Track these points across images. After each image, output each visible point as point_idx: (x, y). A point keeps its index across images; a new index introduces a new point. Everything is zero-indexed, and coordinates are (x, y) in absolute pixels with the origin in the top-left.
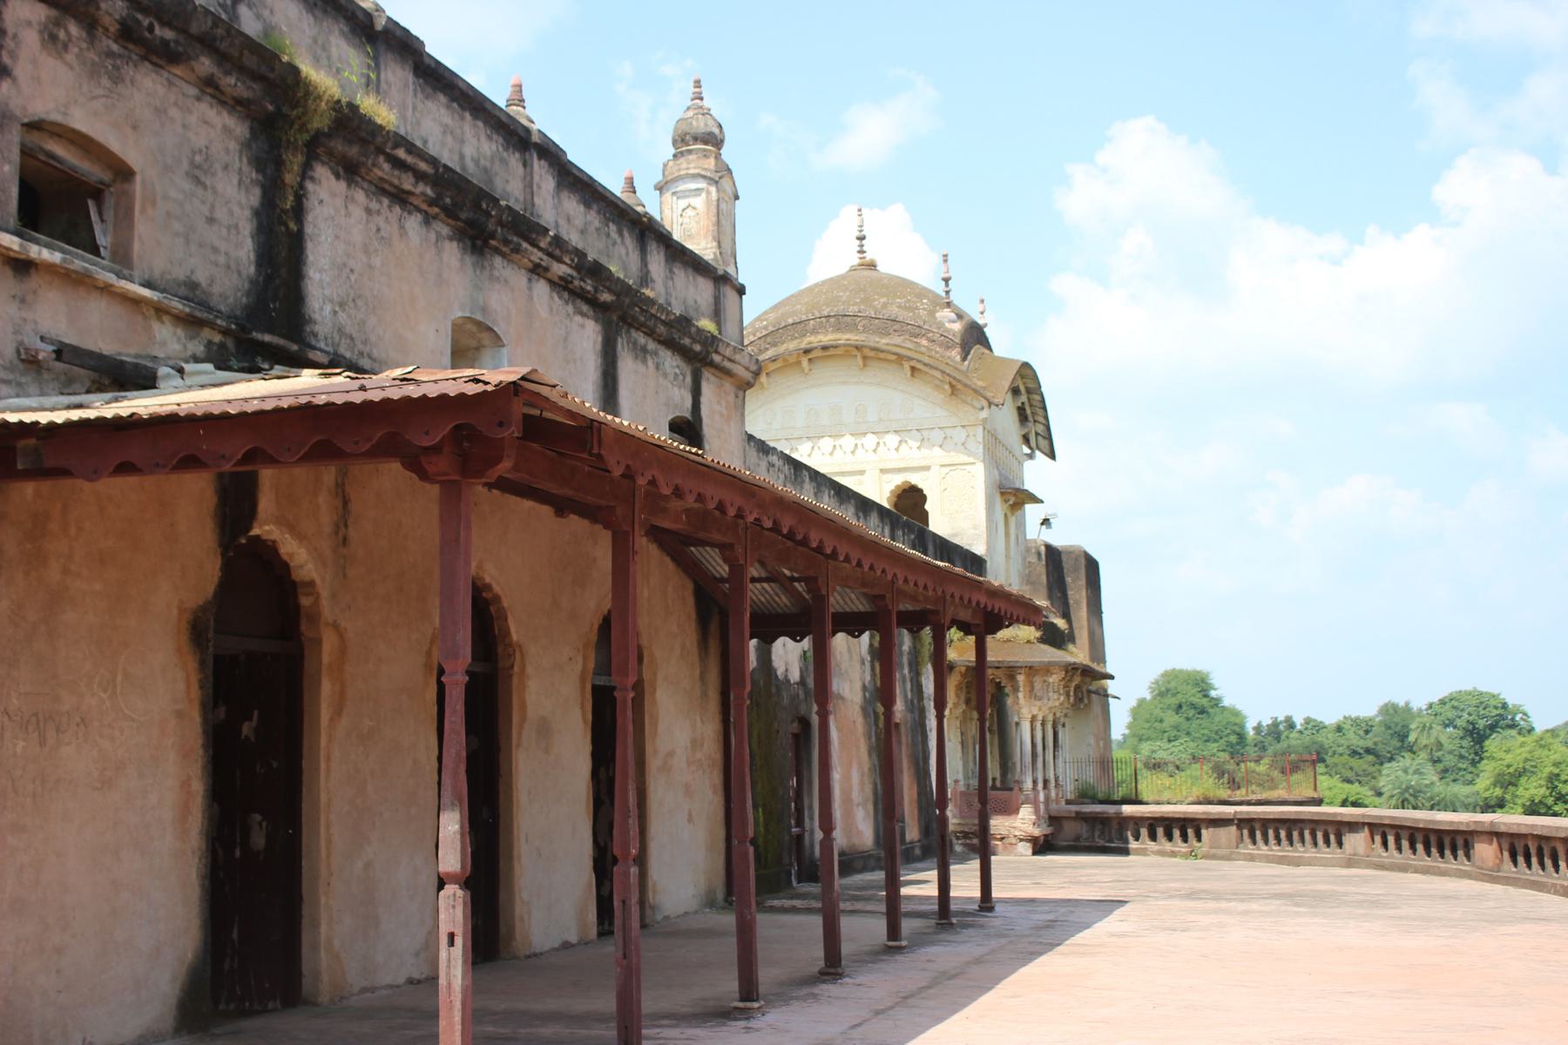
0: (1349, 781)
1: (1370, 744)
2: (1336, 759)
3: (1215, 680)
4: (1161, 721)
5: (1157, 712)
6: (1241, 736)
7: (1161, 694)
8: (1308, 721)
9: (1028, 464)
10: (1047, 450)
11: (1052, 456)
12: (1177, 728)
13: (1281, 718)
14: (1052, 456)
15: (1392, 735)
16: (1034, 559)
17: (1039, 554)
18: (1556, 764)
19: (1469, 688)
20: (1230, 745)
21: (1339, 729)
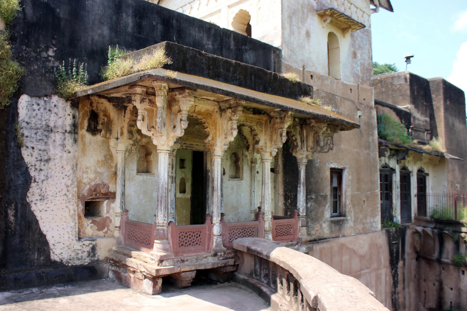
9: (374, 16)
10: (386, 6)
11: (390, 8)
14: (390, 8)
16: (403, 82)
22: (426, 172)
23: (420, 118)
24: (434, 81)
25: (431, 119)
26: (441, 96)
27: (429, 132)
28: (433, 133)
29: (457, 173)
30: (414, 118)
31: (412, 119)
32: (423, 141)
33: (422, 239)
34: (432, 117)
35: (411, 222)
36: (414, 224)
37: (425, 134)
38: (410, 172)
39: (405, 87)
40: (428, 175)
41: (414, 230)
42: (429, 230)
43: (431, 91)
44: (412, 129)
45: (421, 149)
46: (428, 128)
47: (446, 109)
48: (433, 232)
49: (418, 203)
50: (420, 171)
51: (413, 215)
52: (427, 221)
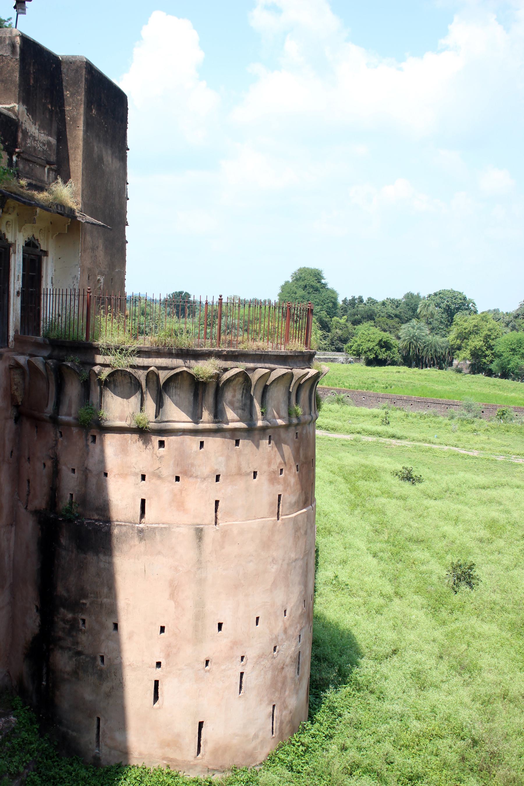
0: (385, 331)
1: (398, 313)
2: (380, 319)
3: (324, 275)
4: (295, 293)
5: (294, 288)
6: (335, 304)
7: (297, 280)
8: (369, 299)
12: (303, 297)
13: (357, 297)
15: (408, 309)
16: (6, 52)
17: (13, 46)
18: (489, 330)
19: (449, 288)
20: (329, 308)
21: (384, 304)
22: (43, 247)
23: (36, 134)
24: (71, 62)
25: (58, 140)
26: (82, 97)
27: (52, 167)
28: (63, 172)
29: (101, 253)
30: (25, 133)
31: (20, 135)
32: (39, 184)
33: (27, 378)
34: (62, 138)
35: (8, 346)
36: (13, 350)
37: (46, 169)
38: (10, 245)
39: (11, 63)
40: (46, 253)
41: (12, 363)
42: (39, 362)
43: (64, 84)
44: (19, 155)
45: (32, 198)
46: (53, 158)
47: (88, 125)
48: (45, 364)
49: (23, 308)
50: (31, 245)
51: (12, 333)
52: (39, 346)
